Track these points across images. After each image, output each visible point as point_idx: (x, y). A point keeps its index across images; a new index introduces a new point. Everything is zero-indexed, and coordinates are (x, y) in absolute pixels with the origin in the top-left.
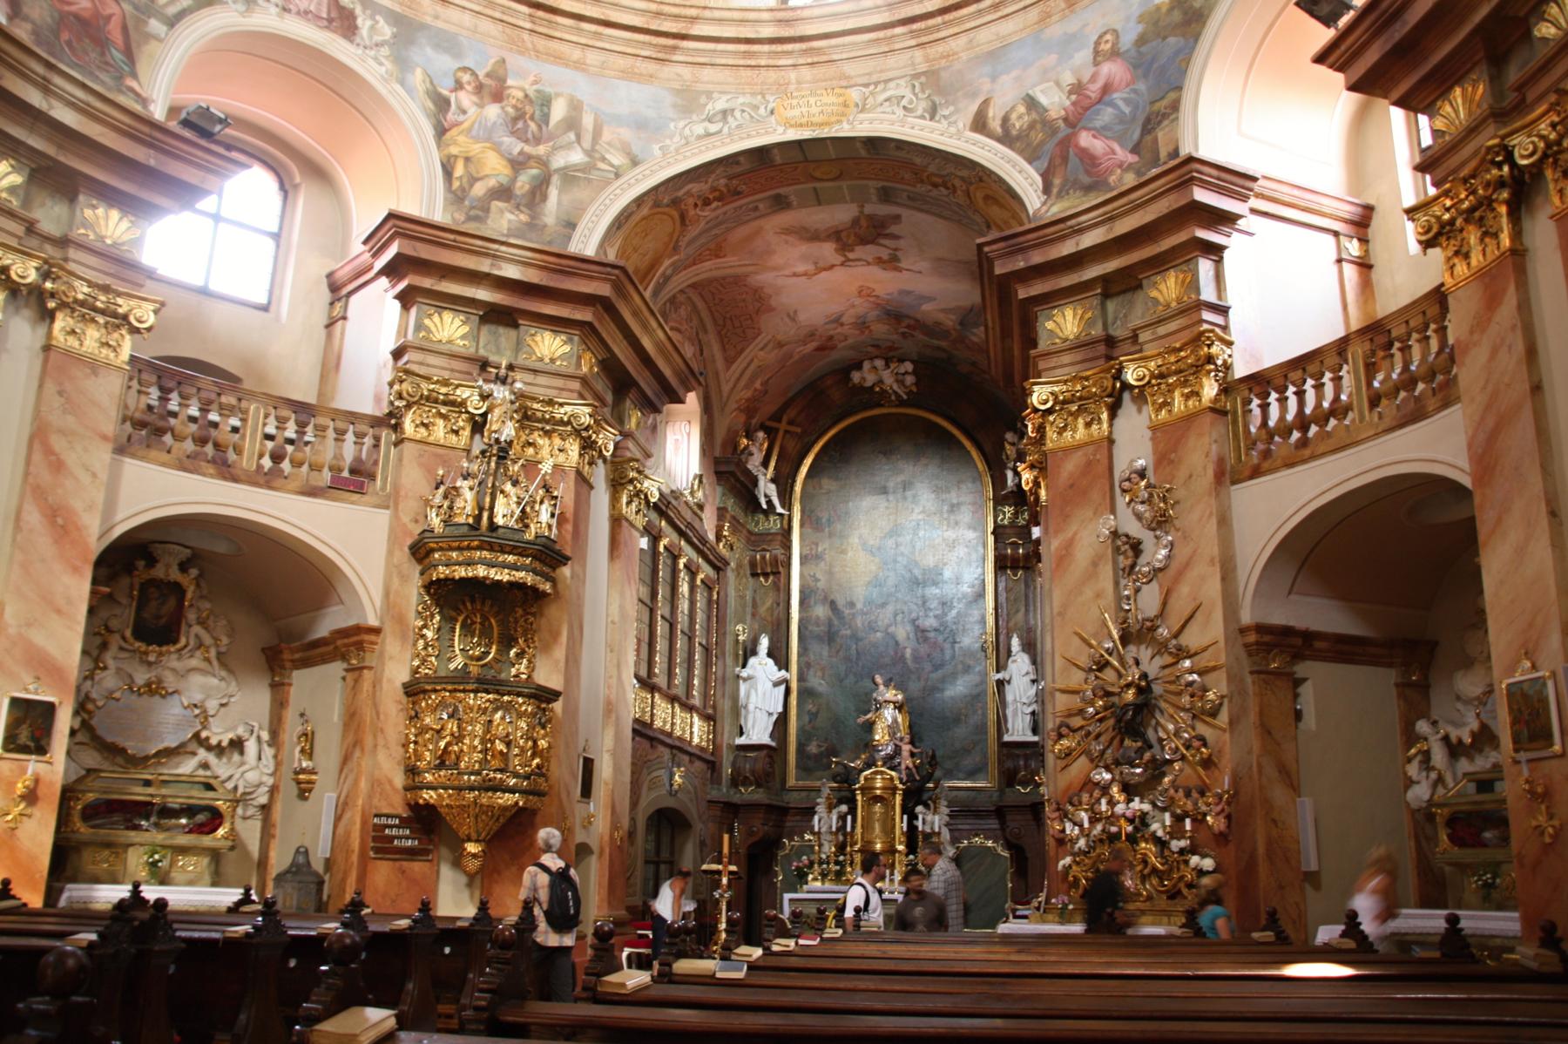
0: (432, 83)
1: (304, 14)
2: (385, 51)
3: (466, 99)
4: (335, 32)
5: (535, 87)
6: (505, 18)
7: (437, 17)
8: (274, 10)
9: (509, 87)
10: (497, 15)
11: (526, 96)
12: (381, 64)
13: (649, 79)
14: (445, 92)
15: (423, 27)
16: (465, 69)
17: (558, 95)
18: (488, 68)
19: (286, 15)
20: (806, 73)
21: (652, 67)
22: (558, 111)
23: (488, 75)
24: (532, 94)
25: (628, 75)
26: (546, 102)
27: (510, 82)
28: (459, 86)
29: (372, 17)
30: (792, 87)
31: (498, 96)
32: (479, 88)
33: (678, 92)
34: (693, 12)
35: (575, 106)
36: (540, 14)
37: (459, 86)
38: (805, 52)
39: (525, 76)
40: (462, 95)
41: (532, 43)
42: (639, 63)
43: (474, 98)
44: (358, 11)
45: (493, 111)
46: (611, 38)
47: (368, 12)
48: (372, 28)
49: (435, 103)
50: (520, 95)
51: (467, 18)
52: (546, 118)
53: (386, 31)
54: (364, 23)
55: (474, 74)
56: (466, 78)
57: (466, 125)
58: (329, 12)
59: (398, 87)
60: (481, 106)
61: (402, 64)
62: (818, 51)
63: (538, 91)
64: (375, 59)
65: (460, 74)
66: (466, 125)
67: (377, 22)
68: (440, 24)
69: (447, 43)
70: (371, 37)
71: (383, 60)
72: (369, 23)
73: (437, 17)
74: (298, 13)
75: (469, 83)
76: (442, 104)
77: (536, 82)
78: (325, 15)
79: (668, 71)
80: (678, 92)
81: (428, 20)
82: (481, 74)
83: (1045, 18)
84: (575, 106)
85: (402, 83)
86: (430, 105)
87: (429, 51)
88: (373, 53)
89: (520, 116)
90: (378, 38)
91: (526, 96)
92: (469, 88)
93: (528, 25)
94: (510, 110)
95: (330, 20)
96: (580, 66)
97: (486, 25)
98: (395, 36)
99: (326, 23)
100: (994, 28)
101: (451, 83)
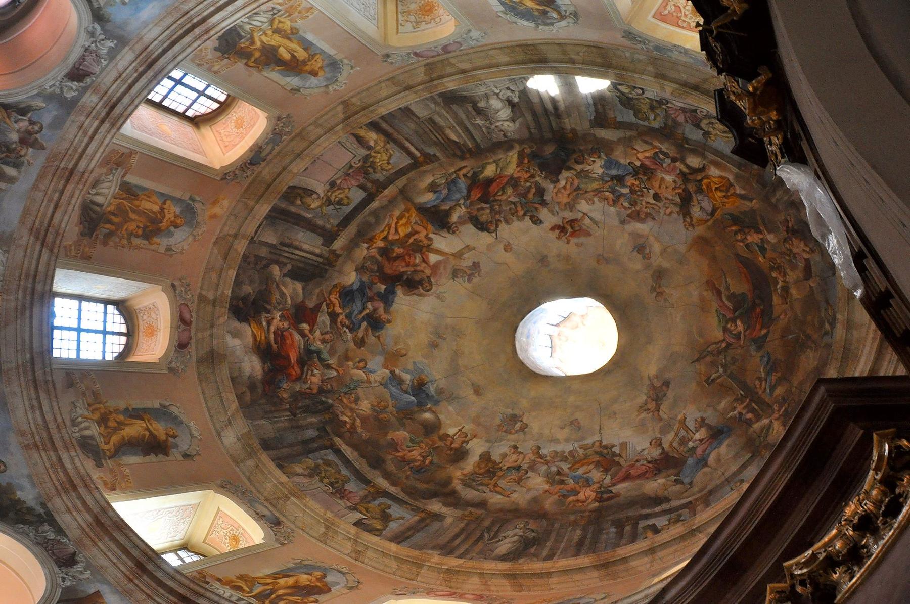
0: (36, 109)
1: (83, 58)
2: (58, 91)
3: (24, 124)
4: (72, 69)
5: (26, 162)
6: (67, 155)
7: (73, 122)
8: (87, 44)
9: (27, 148)
10: (70, 152)
11: (21, 156)
12: (50, 87)
13: (22, 221)
14: (29, 115)
15: (69, 114)
16: (41, 128)
17: (19, 172)
18: (40, 140)
19: (83, 49)
20: (13, 304)
21: (29, 225)
22: (10, 171)
23: (36, 139)
24: (22, 159)
25: (26, 212)
26: (17, 165)
27: (31, 149)
28: (32, 123)
29: (77, 90)
30: (5, 297)
31: (23, 141)
32: (29, 133)
33: (11, 235)
34: (56, 251)
35: (11, 180)
36: (67, 173)
37: (32, 123)
38: (24, 307)
39: (35, 160)
40: (27, 123)
41: (51, 166)
42: (33, 218)
43: (23, 130)
44: (81, 84)
45: (14, 137)
46: (47, 207)
47: (80, 89)
48: (72, 88)
49: (24, 108)
50: (23, 153)
51: (71, 136)
52: (7, 164)
53: (69, 95)
54: (75, 85)
55: (38, 132)
56: (36, 128)
57: (8, 121)
58: (82, 70)
59: (35, 92)
60: (18, 131)
61: (50, 98)
62: (23, 314)
63: (23, 163)
64: (54, 85)
65: (39, 125)
66: (8, 121)
67: (74, 92)
68: (68, 123)
69: (58, 123)
70: (66, 86)
71: (53, 89)
72: (74, 87)
73: (73, 122)
74: (84, 55)
75: (33, 128)
76: (23, 111)
77: (29, 163)
78: (81, 67)
79: (25, 233)
80: (11, 235)
81: (72, 117)
82: (38, 136)
83: (22, 434)
84: (11, 180)
85: (38, 95)
86: (23, 105)
87: (55, 113)
88: (57, 84)
89: (9, 150)
90: (65, 89)
91: (21, 156)
92: (30, 128)
93: (62, 166)
94: (14, 146)
95: (78, 69)
96: (35, 187)
97: (66, 145)
98: (66, 98)
99: (77, 66)
100: (21, 406)
101: (35, 119)
